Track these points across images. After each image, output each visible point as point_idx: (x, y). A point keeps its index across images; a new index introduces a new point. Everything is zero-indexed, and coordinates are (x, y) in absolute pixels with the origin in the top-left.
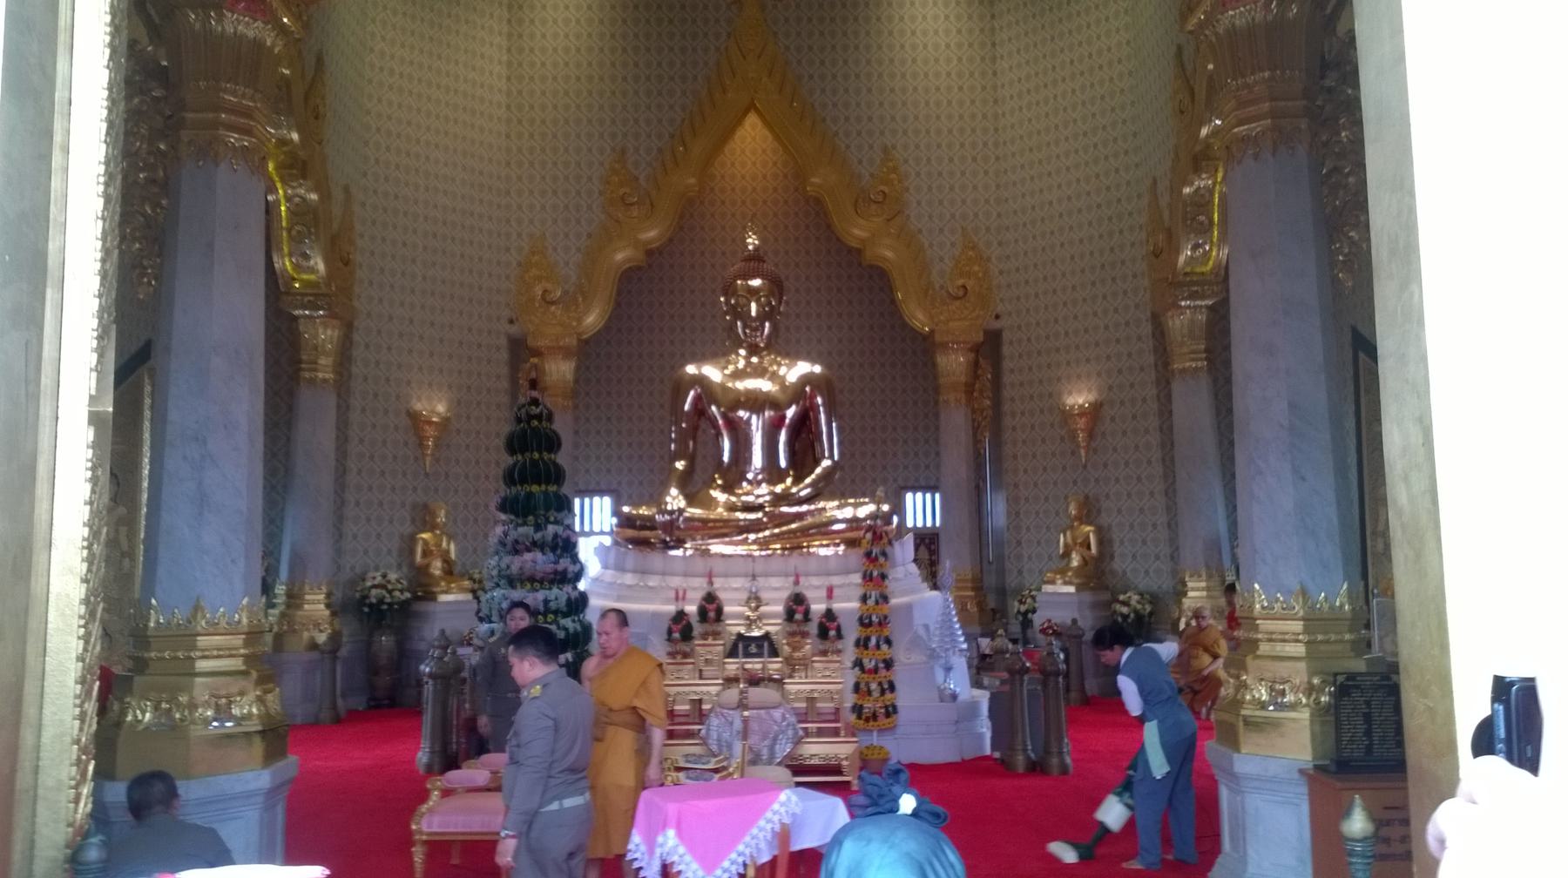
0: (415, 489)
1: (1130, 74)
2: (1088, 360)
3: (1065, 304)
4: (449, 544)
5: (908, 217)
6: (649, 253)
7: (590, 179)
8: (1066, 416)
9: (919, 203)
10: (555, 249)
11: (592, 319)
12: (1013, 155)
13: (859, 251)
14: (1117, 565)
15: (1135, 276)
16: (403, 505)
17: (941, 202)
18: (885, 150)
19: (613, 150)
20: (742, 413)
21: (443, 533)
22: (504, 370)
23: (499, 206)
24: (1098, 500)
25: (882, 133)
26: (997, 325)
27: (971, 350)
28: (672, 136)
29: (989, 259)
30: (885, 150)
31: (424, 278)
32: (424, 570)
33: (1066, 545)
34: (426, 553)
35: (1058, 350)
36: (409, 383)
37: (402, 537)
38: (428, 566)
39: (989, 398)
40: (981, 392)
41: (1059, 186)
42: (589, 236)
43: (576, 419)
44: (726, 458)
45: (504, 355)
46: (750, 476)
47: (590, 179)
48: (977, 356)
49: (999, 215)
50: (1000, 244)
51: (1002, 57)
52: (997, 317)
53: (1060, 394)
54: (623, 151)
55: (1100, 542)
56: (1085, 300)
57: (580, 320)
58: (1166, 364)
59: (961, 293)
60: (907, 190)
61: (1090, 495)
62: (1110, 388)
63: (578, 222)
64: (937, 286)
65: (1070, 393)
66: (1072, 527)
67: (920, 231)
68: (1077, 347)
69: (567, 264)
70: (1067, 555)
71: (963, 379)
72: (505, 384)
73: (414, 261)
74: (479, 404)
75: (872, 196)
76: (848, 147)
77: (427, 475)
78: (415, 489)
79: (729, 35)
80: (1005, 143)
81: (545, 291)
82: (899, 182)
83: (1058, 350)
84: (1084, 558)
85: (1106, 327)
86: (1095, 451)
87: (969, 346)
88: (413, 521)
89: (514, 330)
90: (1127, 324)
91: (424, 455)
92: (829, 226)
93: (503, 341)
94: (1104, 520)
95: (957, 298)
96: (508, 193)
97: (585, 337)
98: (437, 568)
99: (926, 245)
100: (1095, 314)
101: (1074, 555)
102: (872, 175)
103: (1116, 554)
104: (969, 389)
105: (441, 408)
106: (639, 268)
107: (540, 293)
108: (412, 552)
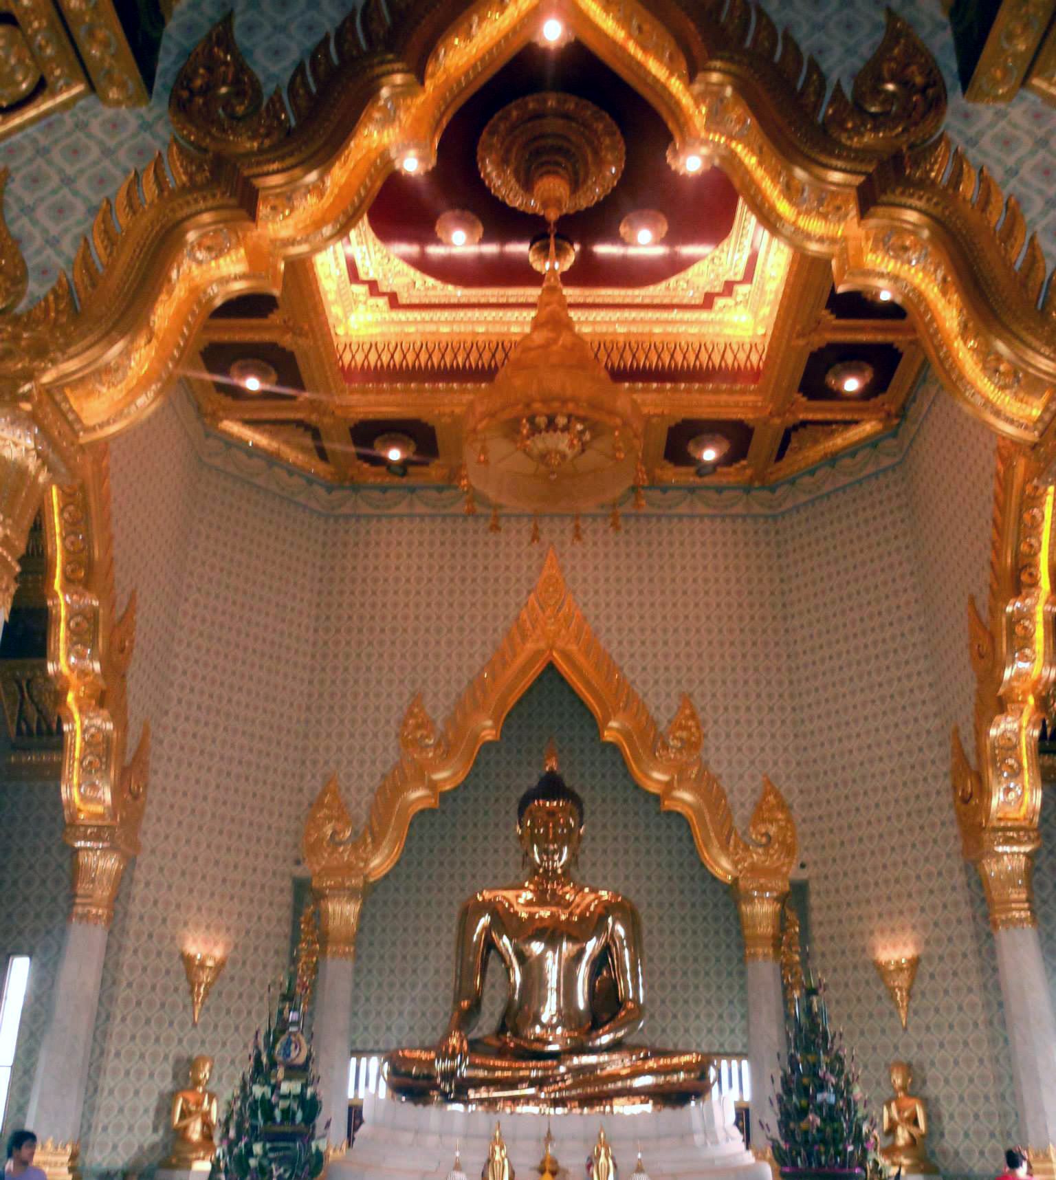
0: (180, 1041)
4: (210, 1102)
5: (707, 762)
6: (444, 797)
7: (388, 722)
8: (880, 970)
9: (718, 749)
10: (348, 789)
11: (379, 863)
13: (657, 798)
14: (948, 1143)
15: (943, 824)
16: (166, 1057)
17: (740, 749)
19: (413, 694)
20: (537, 947)
21: (204, 1092)
22: (286, 913)
23: (296, 748)
24: (922, 1069)
25: (679, 682)
26: (803, 875)
27: (777, 899)
29: (791, 807)
31: (213, 815)
32: (180, 1134)
33: (891, 1120)
34: (185, 1114)
35: (868, 902)
36: (186, 924)
37: (161, 1095)
38: (186, 1128)
39: (796, 952)
40: (789, 946)
42: (384, 776)
43: (357, 971)
44: (516, 997)
45: (288, 898)
46: (545, 1018)
47: (388, 722)
48: (783, 907)
49: (798, 764)
50: (801, 792)
52: (803, 866)
53: (873, 949)
55: (928, 1118)
57: (367, 861)
58: (986, 916)
59: (764, 840)
60: (705, 736)
61: (914, 1062)
62: (927, 943)
63: (373, 762)
64: (740, 833)
65: (885, 948)
66: (896, 1099)
67: (720, 776)
69: (358, 804)
70: (892, 1131)
71: (770, 930)
72: (287, 929)
73: (205, 798)
74: (256, 949)
76: (645, 695)
77: (195, 1025)
78: (180, 1041)
79: (529, 592)
81: (335, 833)
82: (698, 728)
84: (911, 1135)
85: (918, 877)
87: (775, 894)
88: (175, 1077)
89: (299, 871)
90: (940, 874)
91: (193, 1004)
93: (287, 883)
94: (931, 1090)
95: (760, 845)
96: (306, 736)
97: (371, 880)
98: (195, 1131)
99: (727, 790)
101: (900, 1130)
102: (670, 722)
103: (946, 1132)
104: (777, 943)
105: (218, 953)
106: (432, 811)
107: (329, 832)
108: (170, 1112)
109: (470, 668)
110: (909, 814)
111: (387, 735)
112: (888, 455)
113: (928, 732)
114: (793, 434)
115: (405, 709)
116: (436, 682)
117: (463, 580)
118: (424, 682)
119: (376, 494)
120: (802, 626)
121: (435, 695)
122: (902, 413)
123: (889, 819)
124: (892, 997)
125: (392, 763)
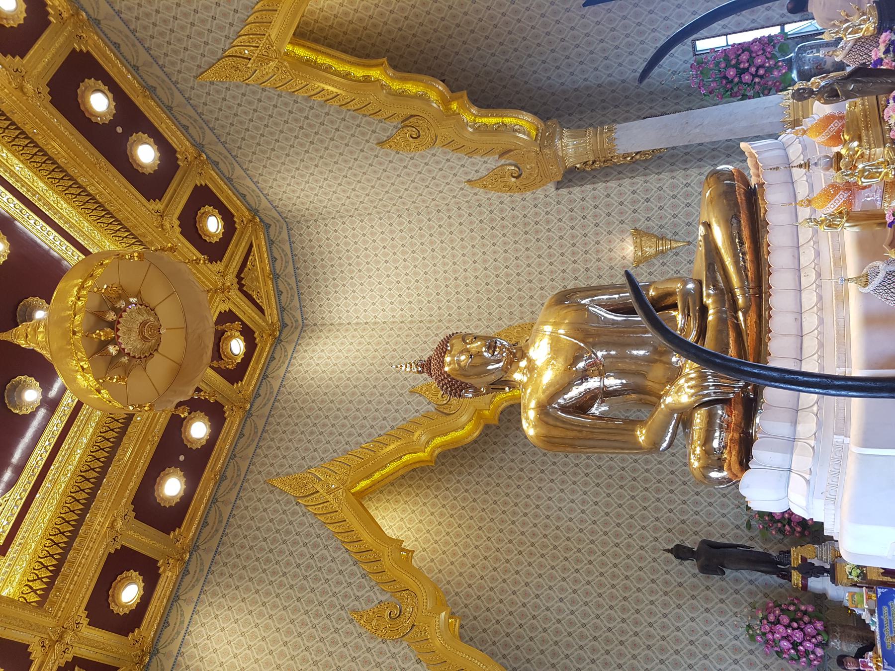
1: (400, 216)
2: (598, 243)
3: (551, 264)
7: (369, 650)
12: (440, 308)
13: (487, 427)
18: (412, 393)
19: (351, 621)
25: (401, 395)
28: (355, 563)
30: (412, 393)
41: (465, 270)
47: (369, 650)
49: (479, 320)
50: (500, 319)
51: (375, 317)
54: (354, 611)
56: (550, 247)
68: (586, 252)
75: (445, 402)
76: (404, 419)
79: (297, 504)
80: (431, 316)
83: (587, 270)
85: (572, 228)
86: (676, 234)
92: (465, 448)
100: (561, 238)
109: (344, 561)
110: (526, 233)
111: (381, 653)
112: (280, 233)
113: (470, 215)
114: (245, 289)
115: (363, 630)
116: (346, 596)
117: (268, 561)
118: (343, 608)
119: (167, 632)
120: (384, 310)
121: (357, 598)
122: (254, 212)
123: (527, 249)
124: (662, 252)
125: (407, 651)
